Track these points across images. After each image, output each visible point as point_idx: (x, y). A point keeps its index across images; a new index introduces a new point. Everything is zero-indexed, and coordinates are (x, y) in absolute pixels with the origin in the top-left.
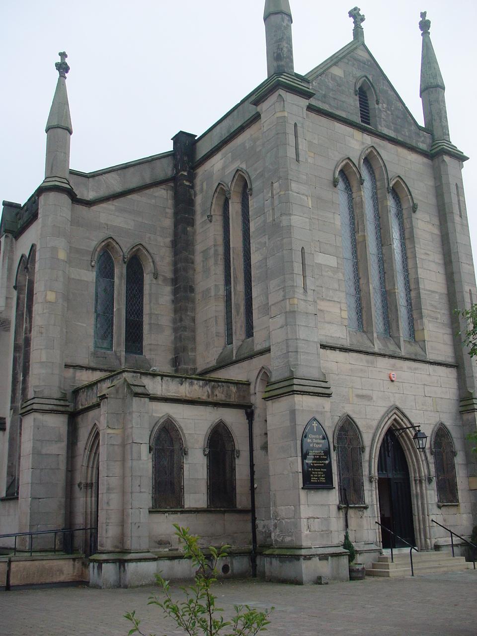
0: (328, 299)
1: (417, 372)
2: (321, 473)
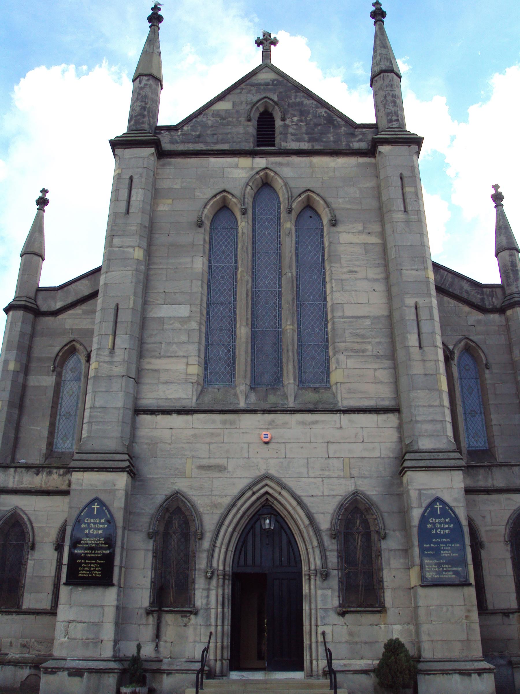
0: (169, 355)
1: (314, 426)
2: (96, 565)
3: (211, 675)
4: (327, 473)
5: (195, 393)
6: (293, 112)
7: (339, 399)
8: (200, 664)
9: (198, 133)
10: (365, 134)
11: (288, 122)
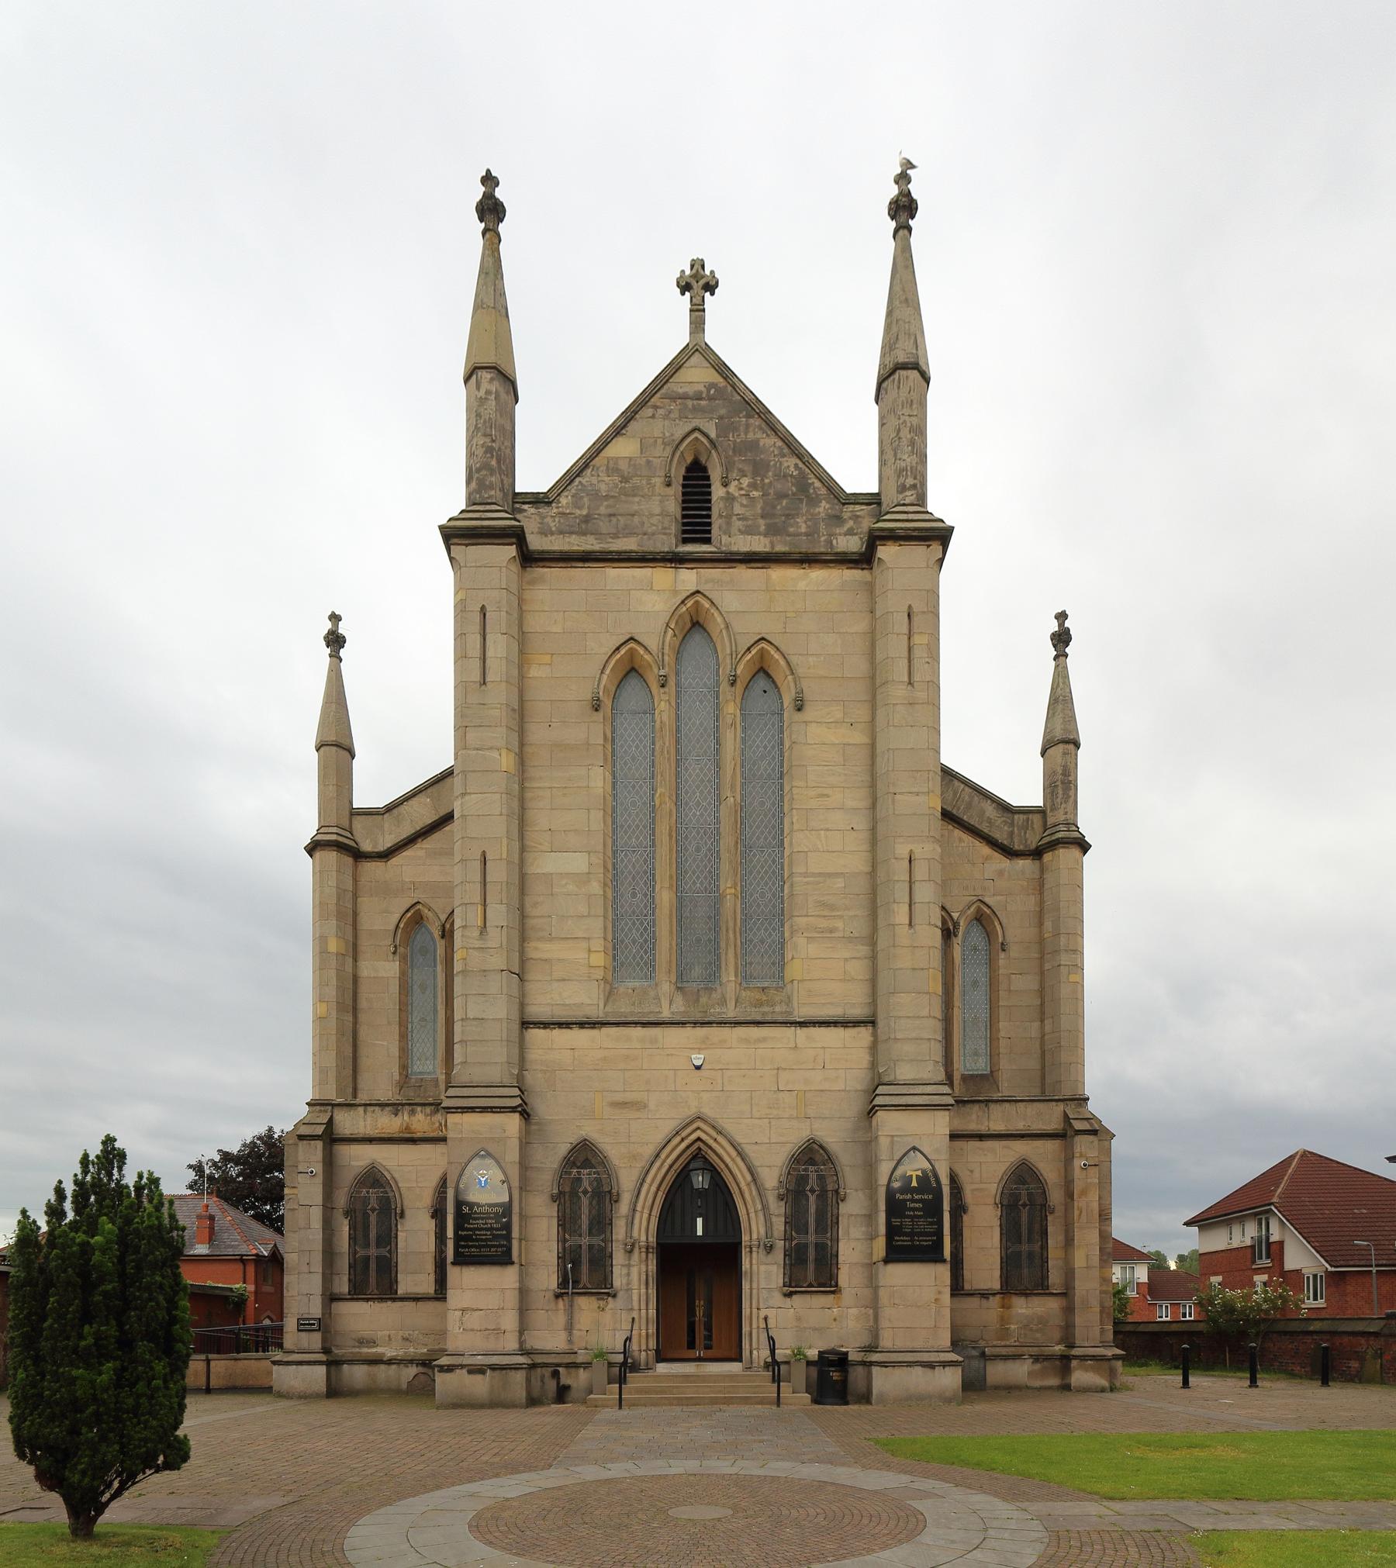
3: (635, 1368)
5: (602, 996)
6: (740, 466)
7: (795, 1004)
8: (622, 1355)
9: (585, 512)
10: (858, 517)
11: (732, 489)
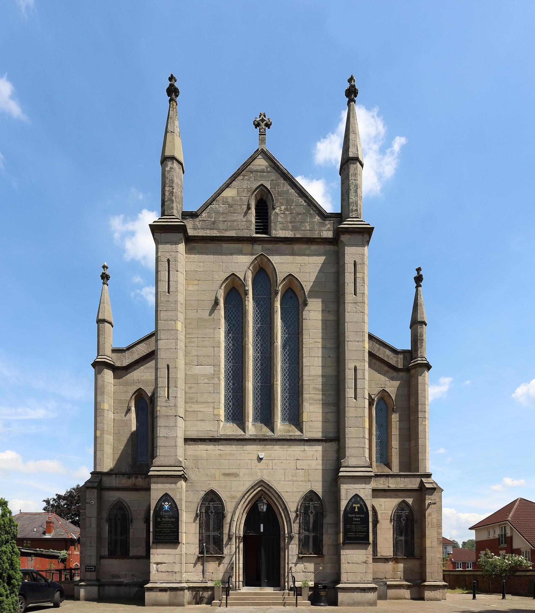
4: (295, 479)
9: (213, 220)
